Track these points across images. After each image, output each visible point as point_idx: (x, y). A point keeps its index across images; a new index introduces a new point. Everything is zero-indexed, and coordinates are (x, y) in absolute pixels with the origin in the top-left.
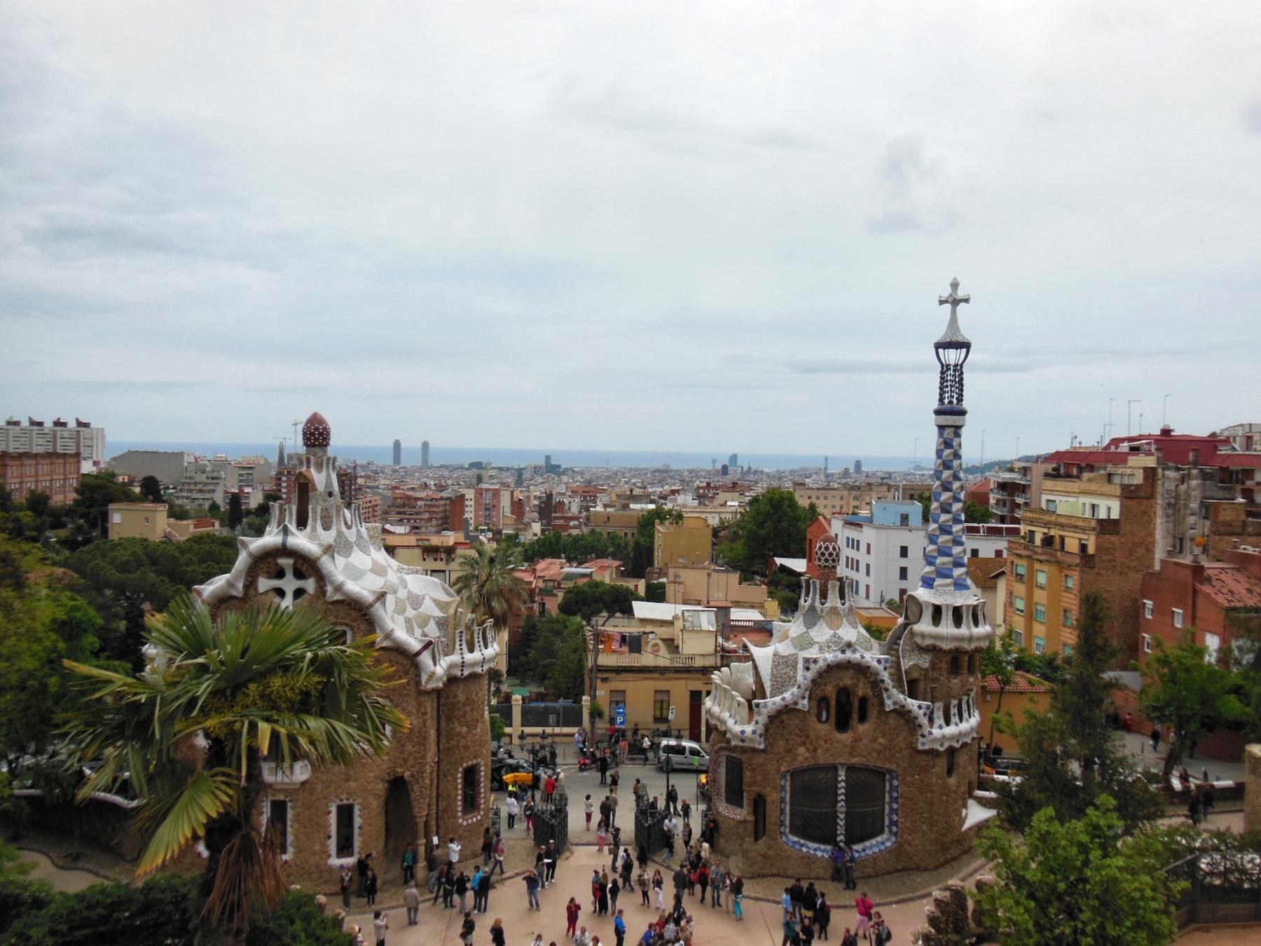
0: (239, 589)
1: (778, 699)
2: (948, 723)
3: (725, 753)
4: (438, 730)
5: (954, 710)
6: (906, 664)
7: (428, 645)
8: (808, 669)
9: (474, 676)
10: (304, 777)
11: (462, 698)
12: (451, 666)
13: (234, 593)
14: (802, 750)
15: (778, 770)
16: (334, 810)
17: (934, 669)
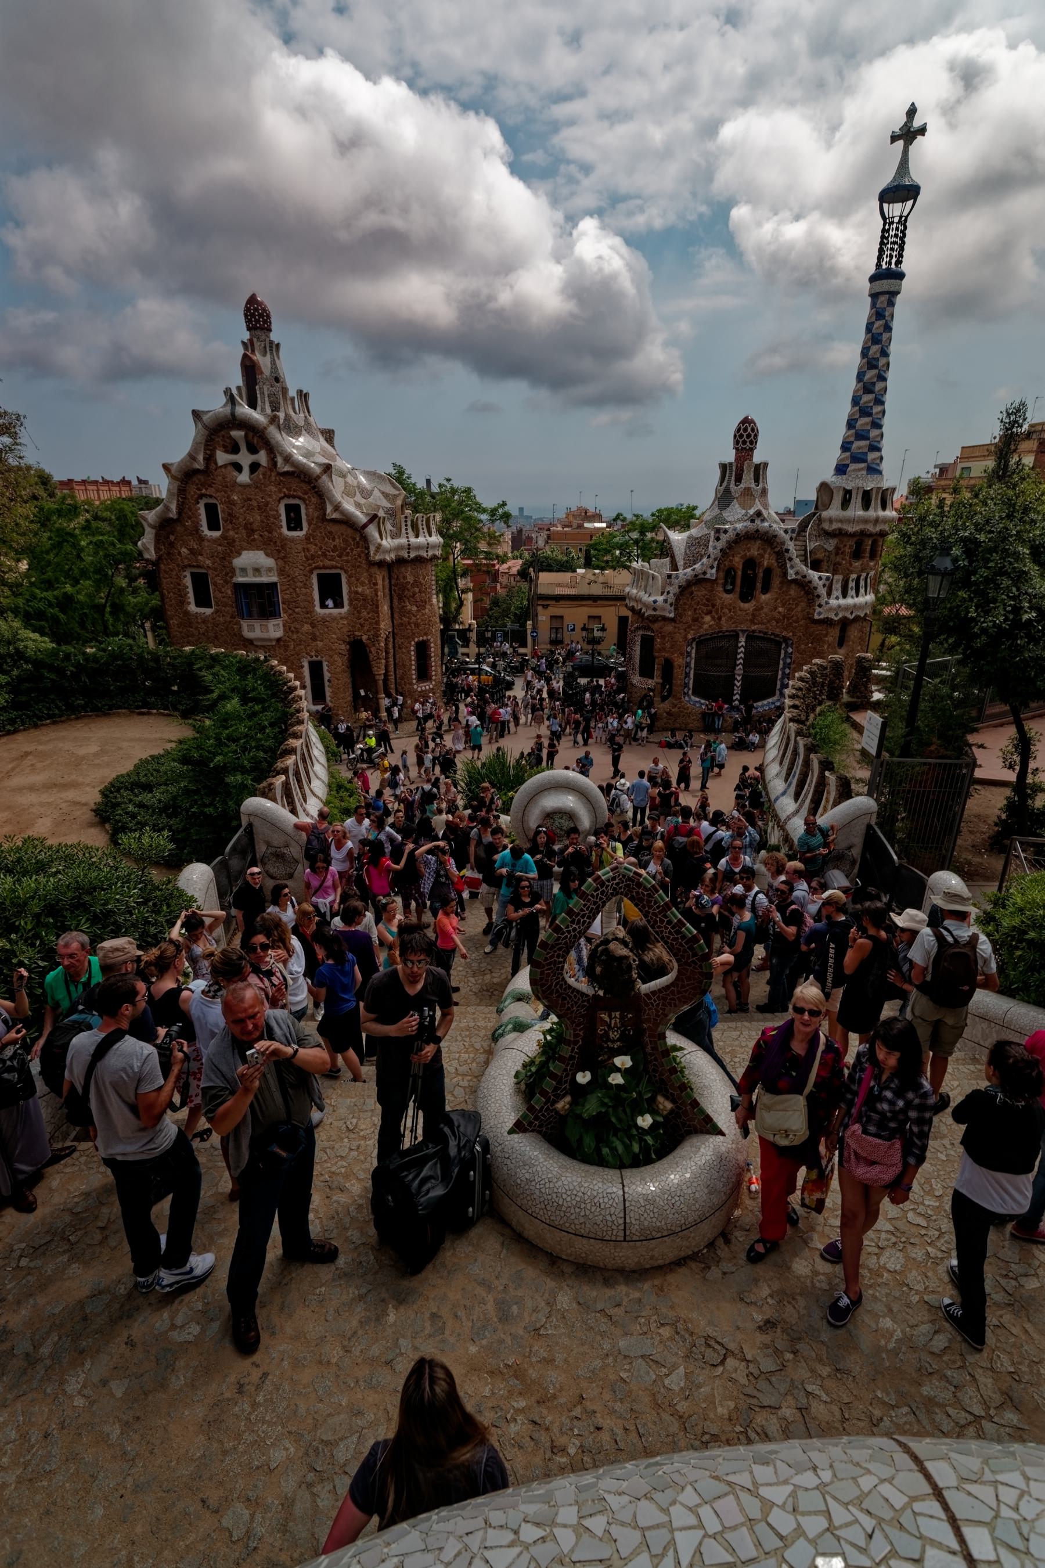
0: (200, 464)
1: (689, 570)
2: (845, 596)
3: (641, 632)
4: (392, 608)
5: (852, 584)
6: (810, 546)
7: (374, 518)
8: (718, 539)
9: (419, 560)
10: (279, 633)
11: (410, 579)
12: (399, 548)
13: (197, 466)
14: (708, 618)
15: (685, 637)
16: (306, 664)
17: (837, 554)
